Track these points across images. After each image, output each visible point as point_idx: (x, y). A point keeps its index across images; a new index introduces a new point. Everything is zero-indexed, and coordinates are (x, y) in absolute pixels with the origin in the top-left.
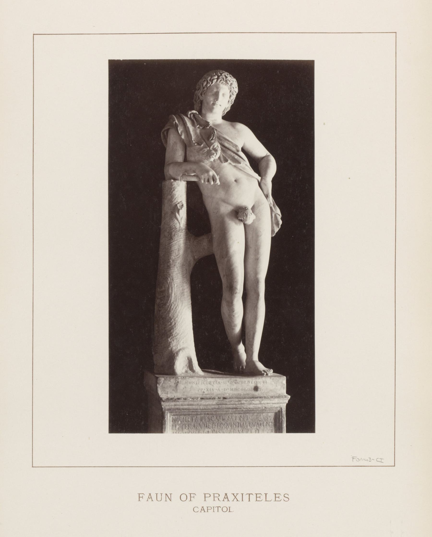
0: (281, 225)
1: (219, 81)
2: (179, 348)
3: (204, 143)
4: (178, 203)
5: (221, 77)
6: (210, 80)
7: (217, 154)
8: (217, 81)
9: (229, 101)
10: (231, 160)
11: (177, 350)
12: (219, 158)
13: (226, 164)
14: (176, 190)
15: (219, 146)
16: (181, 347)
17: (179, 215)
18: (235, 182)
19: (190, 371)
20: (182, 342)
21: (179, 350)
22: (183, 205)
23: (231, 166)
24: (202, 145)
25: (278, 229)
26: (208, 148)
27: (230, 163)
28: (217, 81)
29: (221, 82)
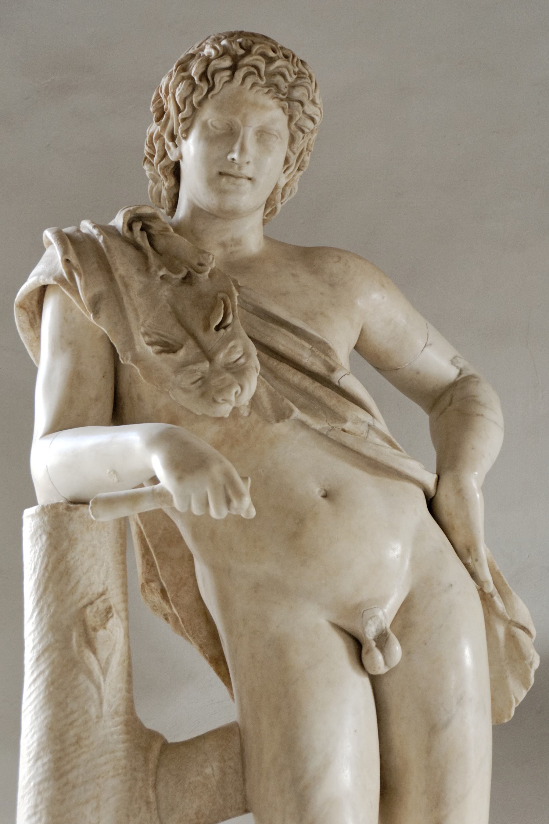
0: (536, 672)
1: (239, 75)
3: (191, 343)
4: (91, 603)
5: (248, 60)
6: (203, 76)
9: (287, 161)
10: (302, 408)
12: (254, 401)
13: (282, 428)
14: (80, 547)
15: (254, 350)
17: (94, 652)
18: (324, 502)
22: (108, 610)
23: (303, 434)
24: (181, 353)
25: (524, 693)
26: (207, 365)
27: (303, 425)
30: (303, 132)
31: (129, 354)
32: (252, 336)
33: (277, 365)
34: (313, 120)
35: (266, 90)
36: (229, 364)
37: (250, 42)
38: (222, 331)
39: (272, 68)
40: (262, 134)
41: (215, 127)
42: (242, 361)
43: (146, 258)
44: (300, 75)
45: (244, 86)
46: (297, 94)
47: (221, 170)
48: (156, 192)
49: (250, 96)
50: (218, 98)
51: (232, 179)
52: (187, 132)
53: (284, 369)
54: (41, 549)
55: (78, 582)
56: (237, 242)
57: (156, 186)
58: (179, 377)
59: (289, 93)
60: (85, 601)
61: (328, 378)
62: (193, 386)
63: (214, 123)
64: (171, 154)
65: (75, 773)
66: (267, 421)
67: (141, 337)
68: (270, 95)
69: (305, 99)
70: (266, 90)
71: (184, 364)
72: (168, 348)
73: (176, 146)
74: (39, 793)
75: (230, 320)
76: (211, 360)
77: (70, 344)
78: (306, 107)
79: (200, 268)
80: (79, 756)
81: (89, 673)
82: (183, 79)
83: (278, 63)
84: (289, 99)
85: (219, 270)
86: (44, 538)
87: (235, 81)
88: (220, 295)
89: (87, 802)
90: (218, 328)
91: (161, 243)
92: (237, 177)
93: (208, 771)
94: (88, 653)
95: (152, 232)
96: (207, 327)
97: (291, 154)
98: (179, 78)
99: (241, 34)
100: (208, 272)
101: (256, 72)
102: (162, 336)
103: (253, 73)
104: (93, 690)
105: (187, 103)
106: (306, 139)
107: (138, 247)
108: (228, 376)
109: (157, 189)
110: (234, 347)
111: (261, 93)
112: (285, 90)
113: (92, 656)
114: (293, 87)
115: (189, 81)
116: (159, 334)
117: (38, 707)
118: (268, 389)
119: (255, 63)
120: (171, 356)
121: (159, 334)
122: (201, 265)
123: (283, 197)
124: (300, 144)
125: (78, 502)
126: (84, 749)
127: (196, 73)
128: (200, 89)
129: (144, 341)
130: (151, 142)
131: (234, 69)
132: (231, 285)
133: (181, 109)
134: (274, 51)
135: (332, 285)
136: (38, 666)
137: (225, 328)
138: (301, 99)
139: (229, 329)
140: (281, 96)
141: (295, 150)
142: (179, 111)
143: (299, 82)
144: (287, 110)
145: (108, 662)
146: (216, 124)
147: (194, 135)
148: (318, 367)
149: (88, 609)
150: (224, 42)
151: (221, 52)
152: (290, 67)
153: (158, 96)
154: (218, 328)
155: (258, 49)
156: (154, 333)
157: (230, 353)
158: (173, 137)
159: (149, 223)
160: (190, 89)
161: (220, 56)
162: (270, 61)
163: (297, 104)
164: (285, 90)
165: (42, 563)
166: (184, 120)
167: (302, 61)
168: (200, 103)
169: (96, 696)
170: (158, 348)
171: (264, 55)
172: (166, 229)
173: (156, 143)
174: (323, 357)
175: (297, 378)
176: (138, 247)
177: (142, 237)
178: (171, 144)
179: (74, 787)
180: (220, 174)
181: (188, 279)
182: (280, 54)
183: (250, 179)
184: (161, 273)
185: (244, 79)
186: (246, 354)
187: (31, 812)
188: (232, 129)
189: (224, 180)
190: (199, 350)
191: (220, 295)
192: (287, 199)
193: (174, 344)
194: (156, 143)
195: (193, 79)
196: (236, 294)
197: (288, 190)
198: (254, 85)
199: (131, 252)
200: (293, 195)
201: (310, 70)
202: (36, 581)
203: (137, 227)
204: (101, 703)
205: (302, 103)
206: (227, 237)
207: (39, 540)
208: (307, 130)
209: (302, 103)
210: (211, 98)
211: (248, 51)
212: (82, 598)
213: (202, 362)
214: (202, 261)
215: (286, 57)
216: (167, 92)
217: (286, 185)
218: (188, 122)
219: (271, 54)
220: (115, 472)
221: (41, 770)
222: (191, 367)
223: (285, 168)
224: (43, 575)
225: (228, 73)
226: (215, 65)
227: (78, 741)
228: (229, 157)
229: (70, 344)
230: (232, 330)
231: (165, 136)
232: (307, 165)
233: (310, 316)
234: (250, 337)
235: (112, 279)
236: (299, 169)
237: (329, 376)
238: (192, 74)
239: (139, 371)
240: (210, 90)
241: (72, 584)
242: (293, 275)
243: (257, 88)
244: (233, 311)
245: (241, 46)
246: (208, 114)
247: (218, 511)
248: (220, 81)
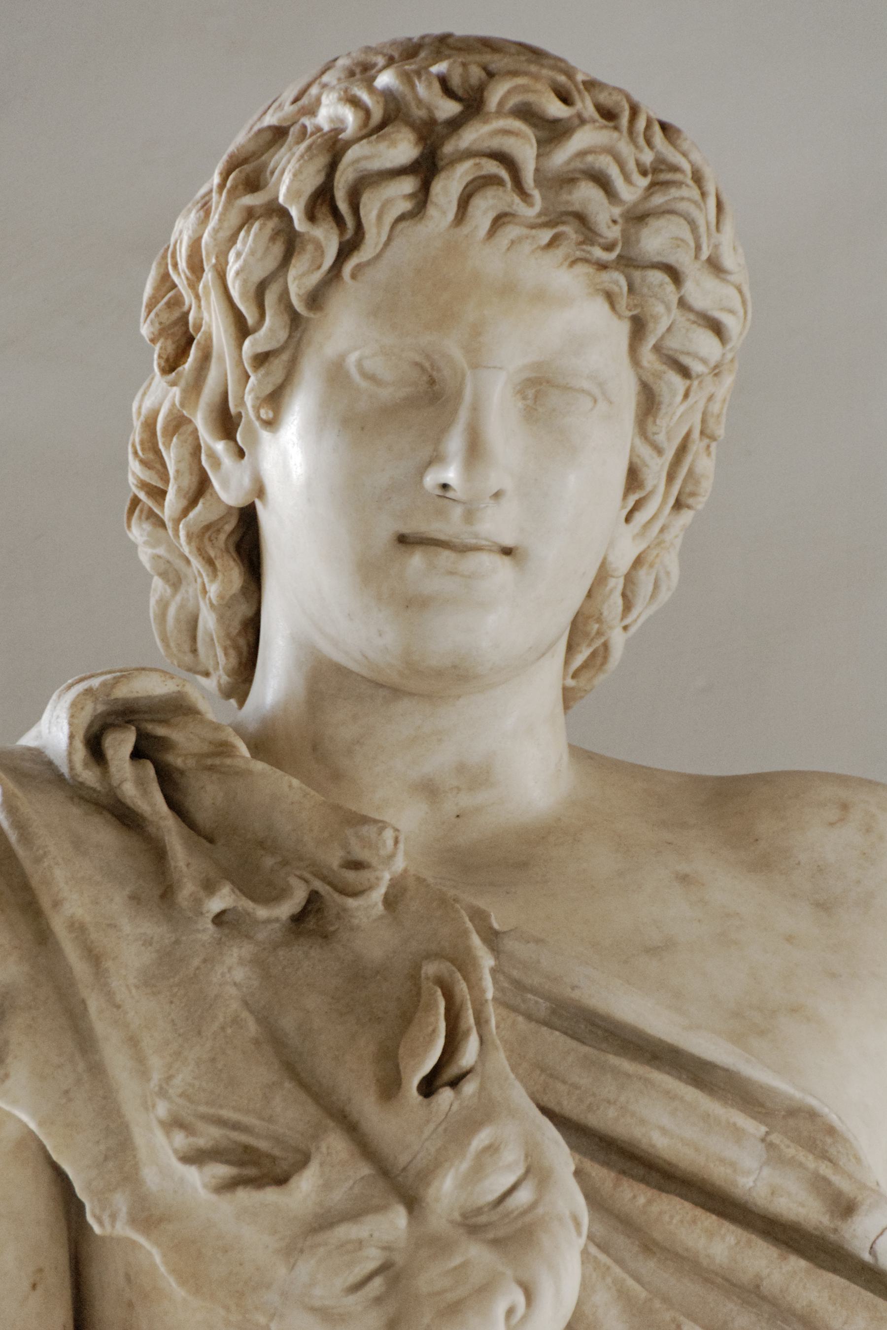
1: (448, 188)
3: (336, 1144)
5: (473, 135)
6: (322, 201)
8: (422, 198)
9: (634, 478)
24: (306, 1185)
26: (398, 1218)
30: (685, 372)
31: (121, 1201)
32: (552, 1105)
33: (649, 1202)
34: (717, 328)
35: (546, 235)
36: (479, 1211)
37: (476, 73)
38: (446, 1095)
39: (562, 156)
40: (541, 390)
41: (371, 378)
42: (524, 1196)
43: (158, 853)
44: (660, 175)
45: (465, 229)
46: (655, 241)
47: (405, 530)
48: (177, 620)
49: (490, 259)
50: (380, 274)
51: (445, 557)
52: (276, 399)
53: (675, 1217)
56: (476, 776)
57: (178, 598)
58: (305, 1268)
59: (627, 240)
61: (832, 1237)
62: (352, 1299)
63: (368, 365)
64: (225, 484)
67: (160, 1136)
68: (560, 252)
69: (683, 259)
70: (546, 235)
72: (258, 1168)
73: (241, 454)
76: (412, 1203)
78: (690, 288)
79: (351, 876)
82: (250, 215)
83: (581, 139)
84: (628, 263)
85: (420, 880)
88: (430, 969)
90: (429, 1087)
91: (207, 796)
92: (464, 549)
95: (176, 760)
96: (389, 1087)
97: (645, 451)
98: (234, 218)
99: (443, 45)
101: (504, 174)
102: (236, 1126)
105: (270, 298)
106: (699, 398)
107: (125, 817)
108: (476, 1254)
109: (182, 607)
110: (492, 1149)
111: (527, 247)
112: (613, 233)
114: (638, 217)
115: (272, 224)
116: (221, 1122)
118: (622, 1294)
119: (496, 143)
120: (270, 1195)
121: (221, 1122)
122: (357, 865)
123: (628, 606)
124: (678, 415)
127: (293, 194)
128: (310, 247)
129: (170, 1153)
130: (151, 444)
131: (426, 168)
132: (465, 933)
133: (250, 321)
134: (566, 99)
135: (824, 907)
137: (455, 1083)
138: (671, 260)
139: (469, 1087)
140: (598, 253)
141: (661, 438)
142: (242, 330)
143: (658, 200)
144: (623, 302)
146: (376, 365)
150: (385, 79)
151: (377, 115)
152: (625, 148)
153: (166, 282)
154: (428, 1087)
155: (509, 92)
156: (204, 1117)
157: (478, 1170)
158: (227, 423)
159: (161, 731)
160: (278, 249)
161: (373, 130)
162: (553, 132)
163: (657, 277)
164: (613, 233)
166: (262, 359)
167: (665, 127)
168: (316, 299)
170: (222, 1171)
171: (527, 113)
172: (223, 749)
173: (168, 447)
174: (811, 1162)
175: (719, 1243)
176: (125, 817)
177: (141, 783)
178: (220, 446)
180: (403, 540)
181: (311, 920)
182: (586, 106)
183: (507, 552)
184: (216, 904)
185: (464, 202)
186: (535, 1171)
188: (432, 382)
189: (417, 560)
190: (366, 1170)
191: (430, 969)
192: (641, 612)
193: (277, 1152)
194: (168, 447)
195: (284, 214)
196: (487, 961)
197: (646, 579)
198: (500, 221)
199: (104, 835)
200: (664, 596)
201: (695, 156)
203: (121, 745)
205: (674, 274)
206: (438, 761)
208: (697, 367)
209: (674, 274)
210: (354, 276)
211: (473, 105)
214: (361, 853)
215: (608, 115)
216: (196, 267)
217: (638, 562)
218: (277, 366)
219: (555, 109)
222: (346, 1232)
223: (631, 503)
225: (408, 185)
226: (357, 161)
228: (431, 480)
230: (482, 1088)
231: (201, 421)
232: (707, 485)
233: (753, 1021)
234: (546, 1111)
235: (43, 937)
236: (679, 505)
237: (835, 1230)
238: (281, 200)
239: (158, 1259)
240: (346, 250)
242: (684, 879)
243: (511, 232)
244: (481, 1022)
245: (446, 87)
246: (346, 334)
248: (380, 217)
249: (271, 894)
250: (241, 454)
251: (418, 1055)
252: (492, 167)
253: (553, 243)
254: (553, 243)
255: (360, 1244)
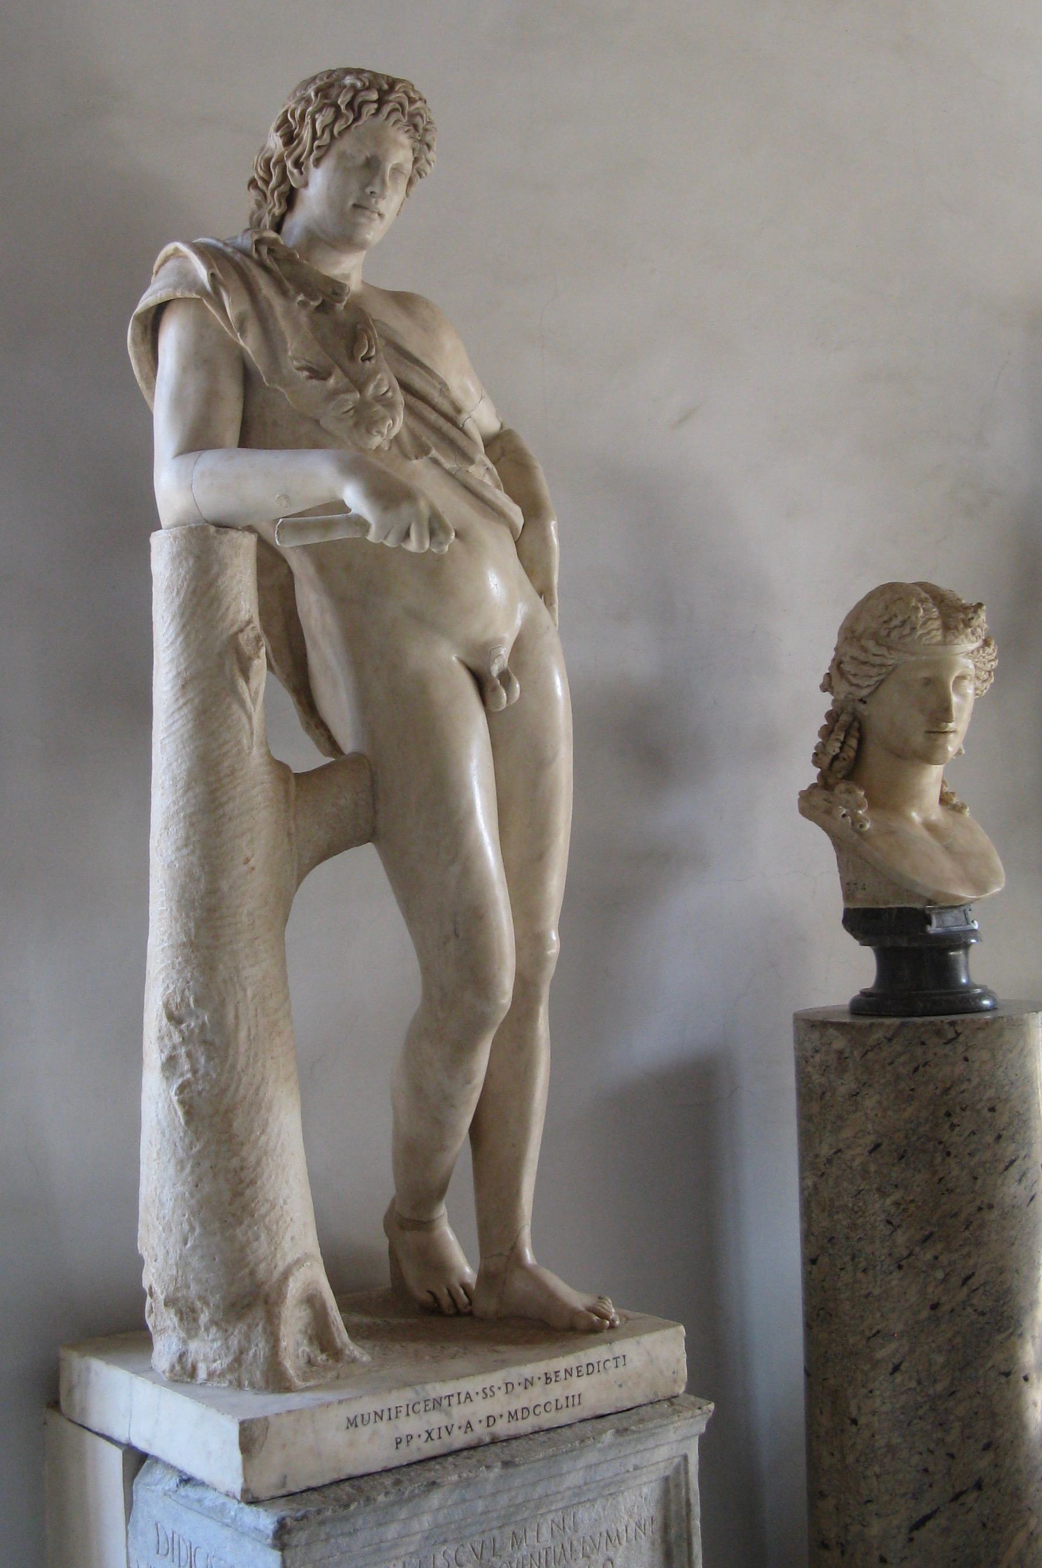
2: (281, 1268)
3: (338, 371)
4: (242, 631)
5: (392, 97)
6: (350, 105)
7: (394, 421)
8: (378, 111)
11: (276, 1275)
14: (229, 572)
16: (290, 1259)
17: (247, 680)
19: (321, 1358)
20: (288, 1237)
21: (286, 1276)
24: (332, 381)
28: (378, 111)
29: (392, 119)
39: (413, 108)
42: (390, 394)
52: (317, 162)
54: (187, 572)
55: (228, 609)
60: (235, 628)
64: (295, 181)
65: (231, 805)
66: (407, 457)
70: (407, 128)
71: (335, 393)
72: (318, 374)
73: (301, 173)
74: (192, 824)
75: (373, 353)
77: (206, 361)
79: (335, 297)
80: (235, 787)
81: (242, 704)
86: (191, 562)
87: (381, 116)
89: (243, 834)
90: (364, 359)
93: (342, 802)
94: (241, 682)
100: (344, 303)
103: (397, 110)
104: (244, 719)
108: (378, 407)
110: (382, 379)
111: (401, 131)
113: (244, 684)
115: (333, 110)
117: (185, 736)
122: (336, 294)
125: (223, 526)
126: (239, 781)
127: (342, 103)
131: (381, 102)
133: (319, 133)
136: (184, 695)
139: (373, 361)
145: (257, 693)
147: (328, 163)
148: (447, 408)
149: (240, 636)
157: (378, 386)
158: (297, 164)
161: (368, 89)
165: (188, 586)
166: (319, 147)
168: (340, 133)
169: (247, 726)
170: (306, 373)
173: (274, 168)
175: (433, 417)
178: (295, 171)
179: (230, 819)
181: (324, 308)
185: (389, 114)
187: (180, 843)
194: (274, 168)
202: (180, 605)
203: (264, 250)
204: (252, 734)
207: (184, 562)
212: (232, 625)
213: (353, 391)
220: (286, 497)
221: (193, 801)
224: (191, 600)
225: (375, 106)
227: (233, 772)
228: (368, 190)
229: (206, 361)
231: (289, 164)
240: (355, 120)
241: (223, 610)
243: (398, 125)
247: (421, 543)
249: (314, 299)
250: (301, 173)
251: (360, 350)
252: (398, 106)
253: (407, 132)
254: (407, 132)
255: (347, 400)
